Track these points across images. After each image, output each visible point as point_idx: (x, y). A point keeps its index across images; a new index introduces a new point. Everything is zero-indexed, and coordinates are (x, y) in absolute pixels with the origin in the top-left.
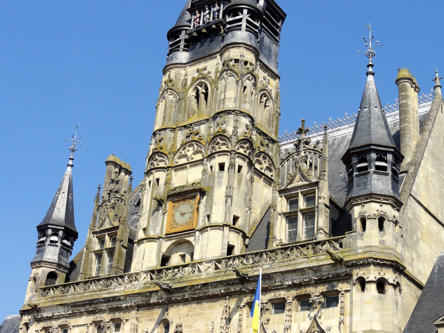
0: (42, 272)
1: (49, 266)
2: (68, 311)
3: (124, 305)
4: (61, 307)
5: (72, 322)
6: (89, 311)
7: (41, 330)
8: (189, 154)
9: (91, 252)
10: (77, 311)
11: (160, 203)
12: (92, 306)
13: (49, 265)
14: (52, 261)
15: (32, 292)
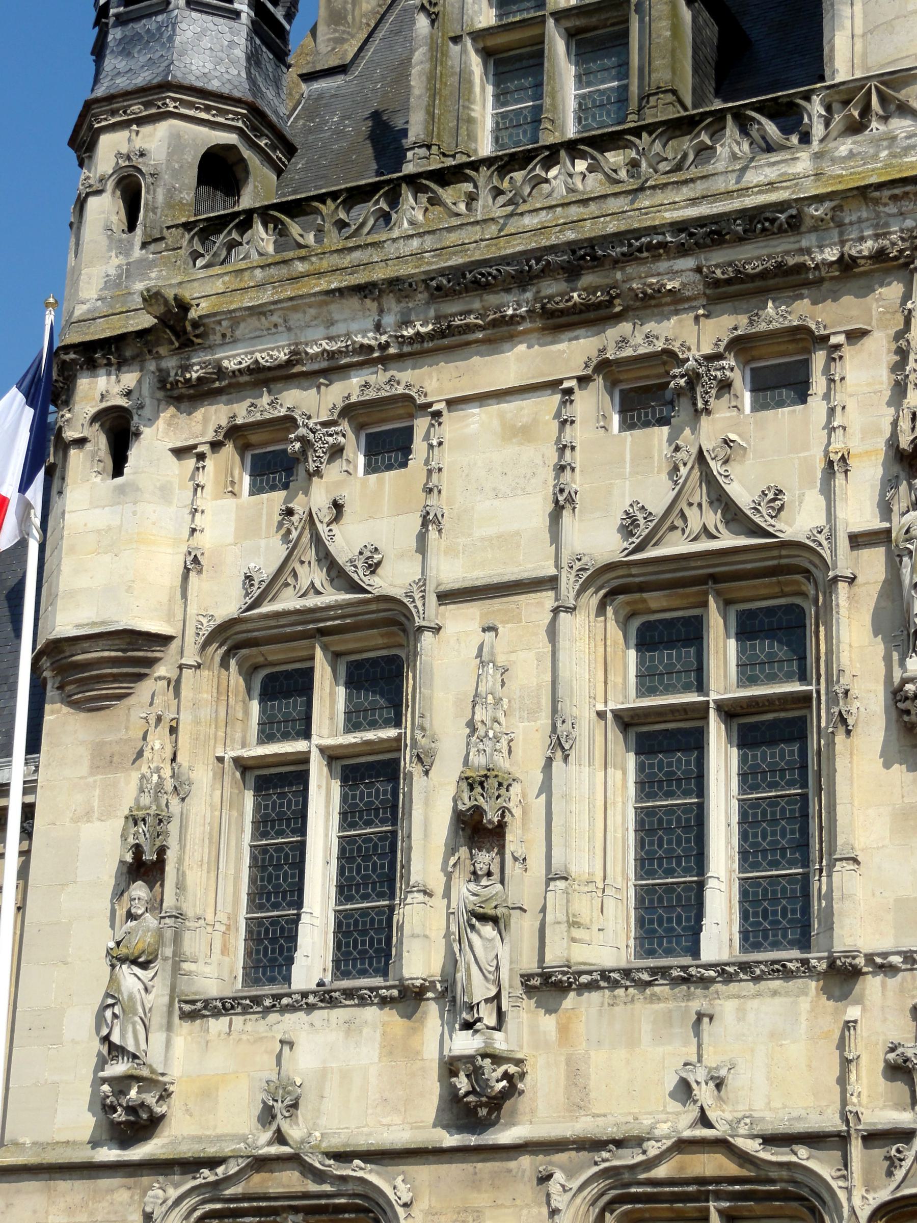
0: (168, 146)
1: (203, 115)
2: (407, 323)
3: (831, 254)
4: (354, 302)
5: (434, 381)
6: (562, 312)
7: (216, 446)
9: (456, 39)
10: (471, 319)
12: (588, 279)
13: (208, 109)
14: (225, 90)
15: (124, 250)
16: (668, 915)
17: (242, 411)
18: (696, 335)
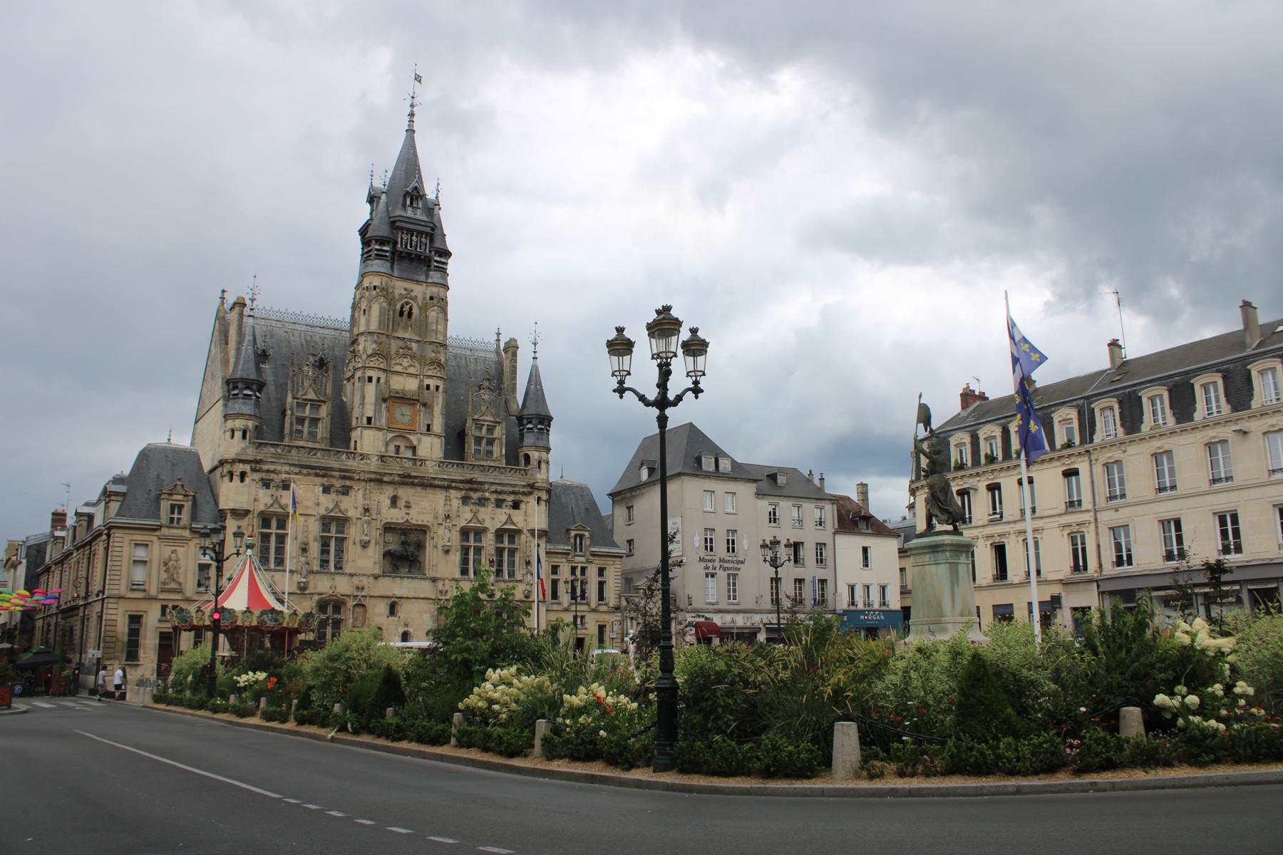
8: (405, 364)
11: (384, 400)
16: (324, 563)
17: (264, 475)
18: (338, 484)
